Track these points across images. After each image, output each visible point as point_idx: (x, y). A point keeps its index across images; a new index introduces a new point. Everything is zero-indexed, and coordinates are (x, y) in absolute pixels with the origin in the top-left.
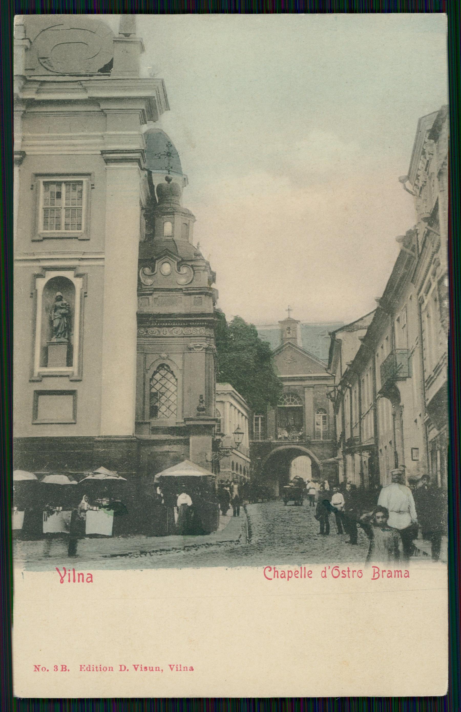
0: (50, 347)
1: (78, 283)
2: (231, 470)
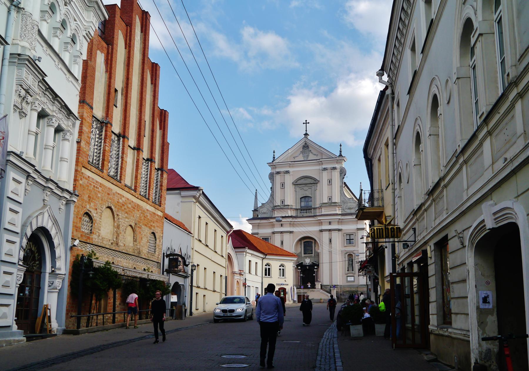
1: (354, 255)
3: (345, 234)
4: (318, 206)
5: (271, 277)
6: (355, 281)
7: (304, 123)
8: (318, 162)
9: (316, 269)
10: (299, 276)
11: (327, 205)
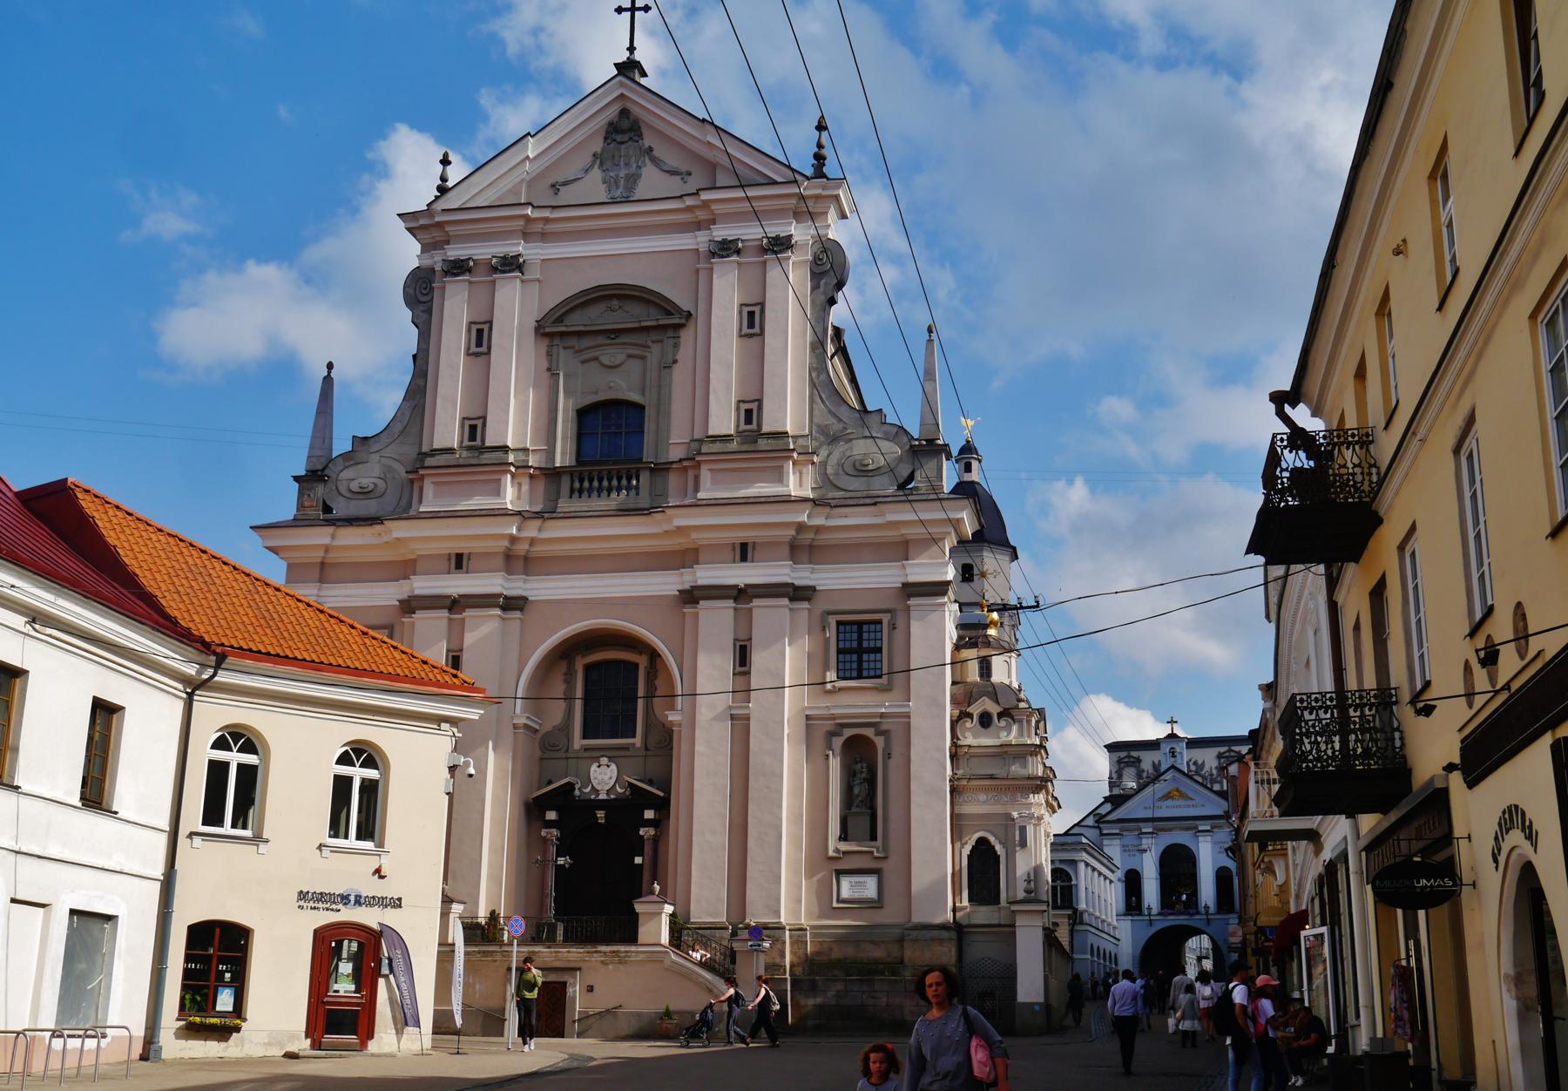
0: (849, 819)
1: (880, 742)
2: (1089, 956)
3: (832, 620)
4: (675, 454)
5: (258, 839)
6: (887, 900)
7: (619, 10)
8: (689, 209)
9: (649, 823)
10: (543, 864)
11: (734, 446)
